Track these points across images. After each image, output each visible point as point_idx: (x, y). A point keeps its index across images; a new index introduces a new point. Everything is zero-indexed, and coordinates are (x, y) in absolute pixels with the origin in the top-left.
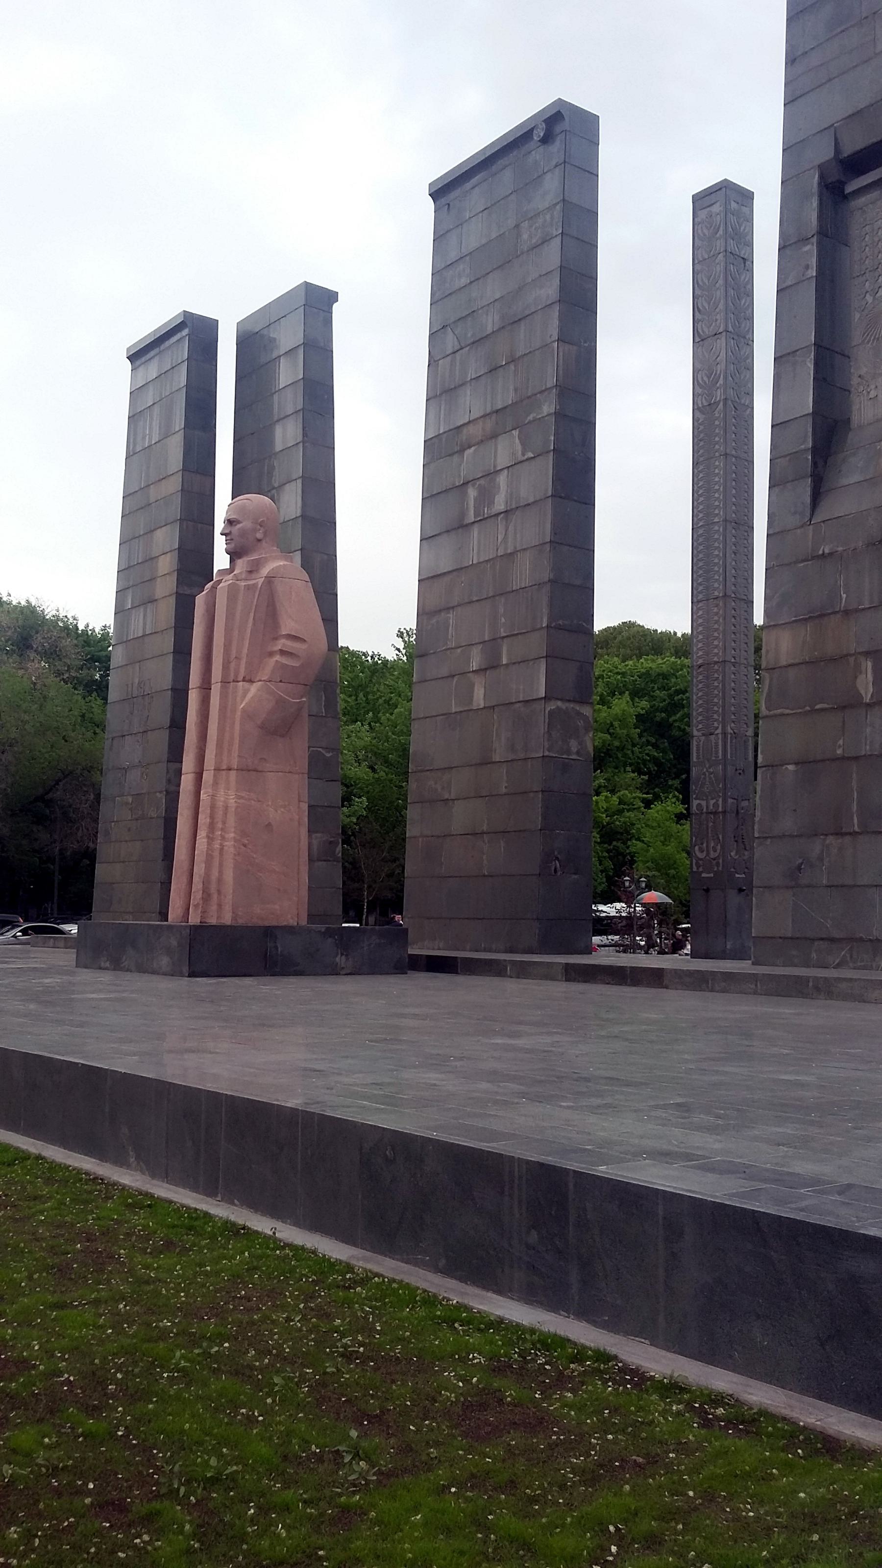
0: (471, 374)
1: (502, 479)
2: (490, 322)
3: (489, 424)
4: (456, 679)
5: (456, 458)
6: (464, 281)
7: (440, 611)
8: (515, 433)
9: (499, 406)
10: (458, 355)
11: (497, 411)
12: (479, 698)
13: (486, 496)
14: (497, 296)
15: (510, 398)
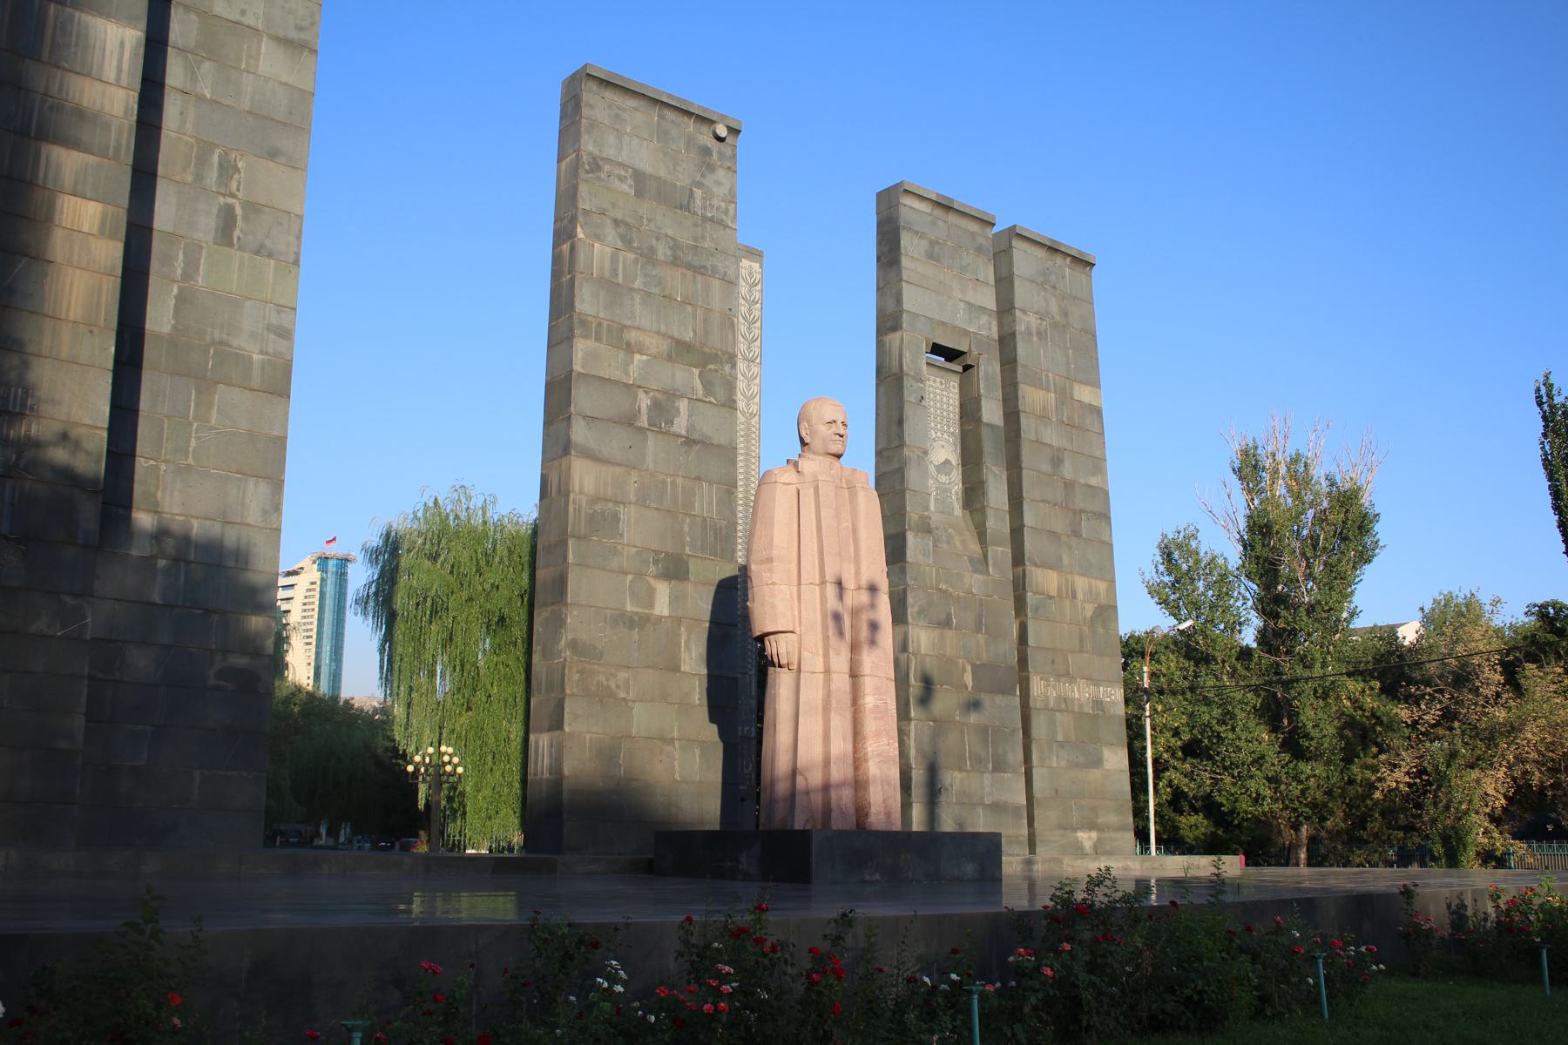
0: (637, 285)
1: (683, 405)
2: (662, 252)
3: (664, 346)
4: (630, 577)
5: (621, 355)
6: (625, 187)
7: (607, 500)
8: (696, 371)
9: (676, 335)
10: (621, 255)
11: (672, 338)
12: (662, 607)
13: (663, 410)
14: (670, 233)
15: (688, 336)
